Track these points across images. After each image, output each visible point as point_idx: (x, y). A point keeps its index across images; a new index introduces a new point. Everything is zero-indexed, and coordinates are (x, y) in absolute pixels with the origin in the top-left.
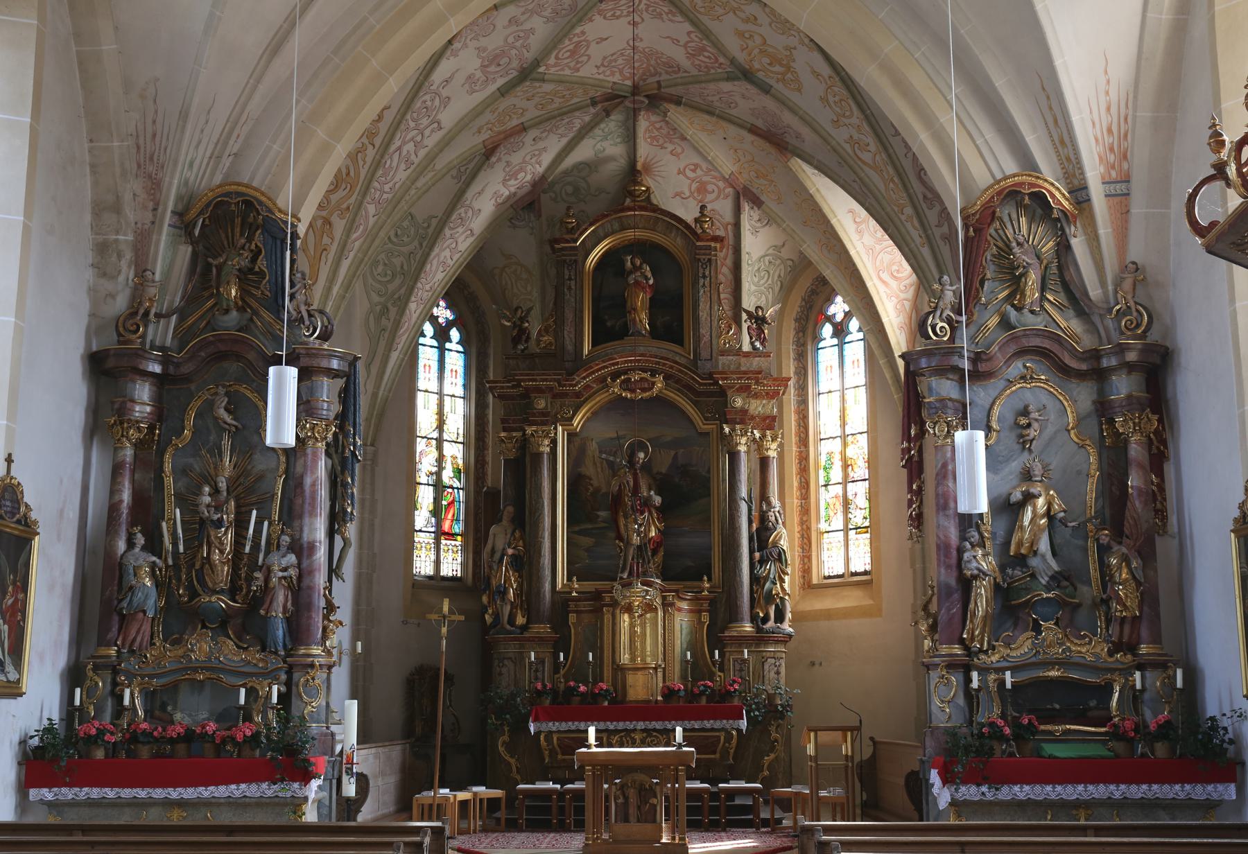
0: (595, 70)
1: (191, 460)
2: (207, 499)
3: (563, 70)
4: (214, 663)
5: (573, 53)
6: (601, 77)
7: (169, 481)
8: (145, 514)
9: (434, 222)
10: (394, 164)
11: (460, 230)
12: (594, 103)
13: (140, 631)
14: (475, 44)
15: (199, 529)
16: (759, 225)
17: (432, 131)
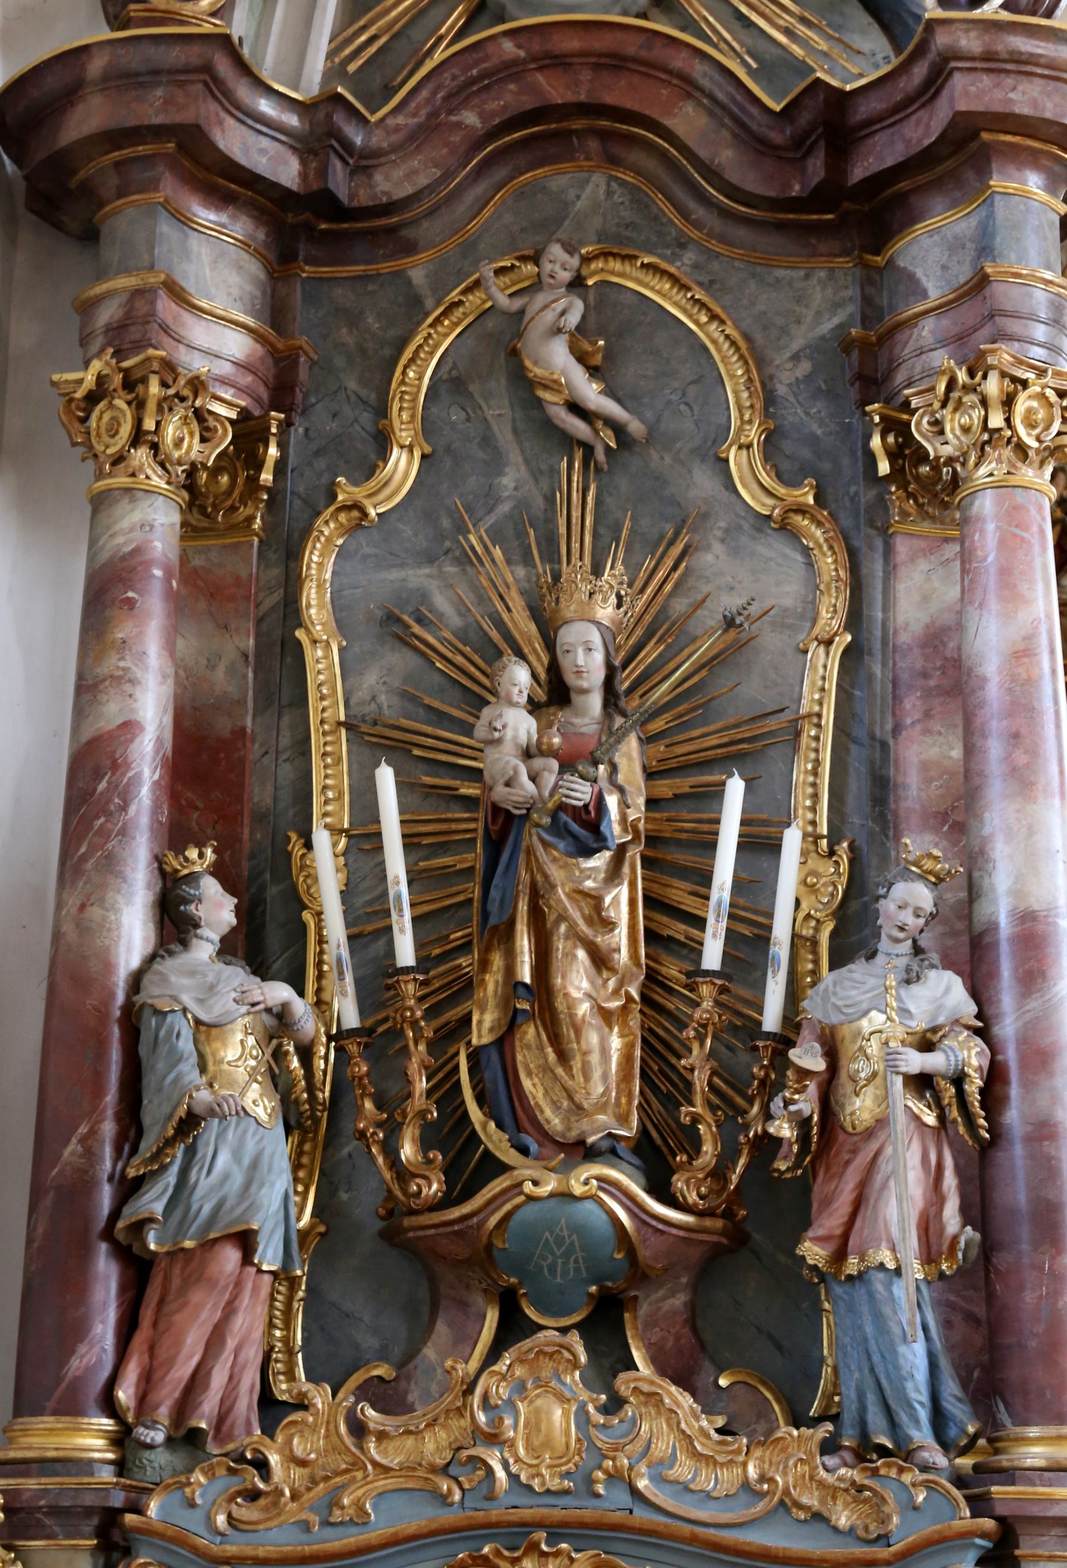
1: (418, 576)
2: (520, 725)
4: (612, 1501)
7: (323, 661)
8: (228, 793)
13: (235, 1331)
15: (485, 857)
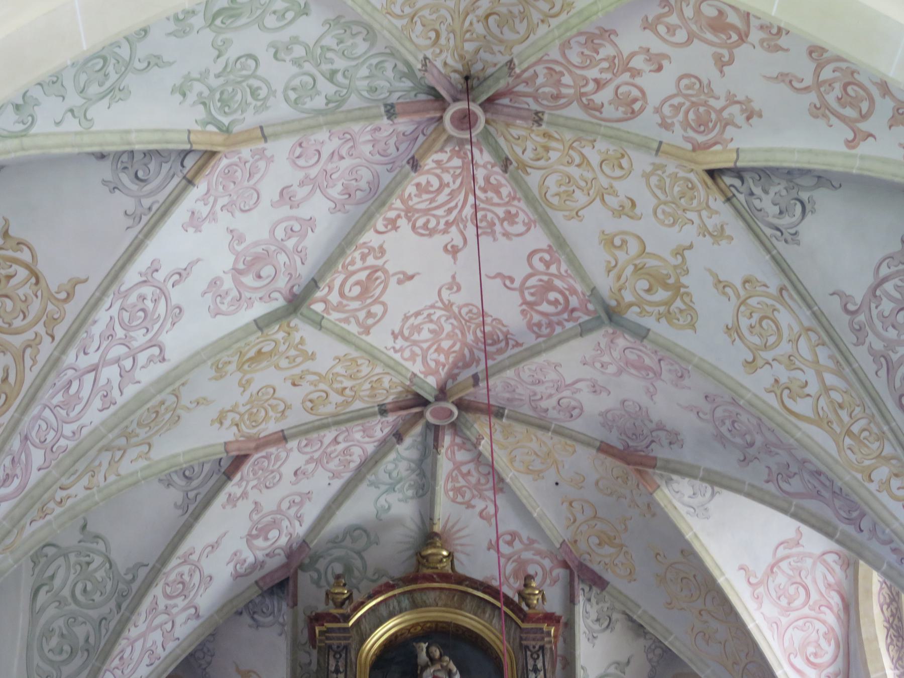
0: (390, 343)
3: (346, 320)
5: (365, 288)
6: (397, 356)
9: (142, 573)
10: (85, 394)
11: (180, 602)
12: (383, 411)
14: (225, 219)
16: (596, 627)
17: (150, 360)
